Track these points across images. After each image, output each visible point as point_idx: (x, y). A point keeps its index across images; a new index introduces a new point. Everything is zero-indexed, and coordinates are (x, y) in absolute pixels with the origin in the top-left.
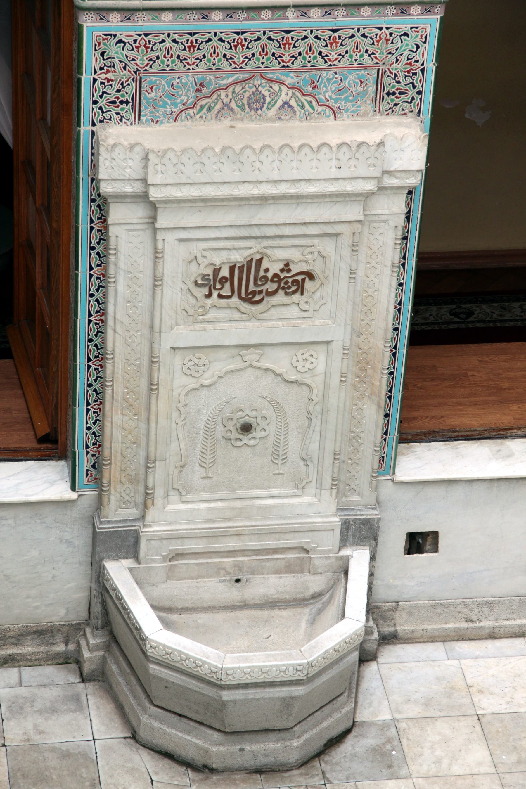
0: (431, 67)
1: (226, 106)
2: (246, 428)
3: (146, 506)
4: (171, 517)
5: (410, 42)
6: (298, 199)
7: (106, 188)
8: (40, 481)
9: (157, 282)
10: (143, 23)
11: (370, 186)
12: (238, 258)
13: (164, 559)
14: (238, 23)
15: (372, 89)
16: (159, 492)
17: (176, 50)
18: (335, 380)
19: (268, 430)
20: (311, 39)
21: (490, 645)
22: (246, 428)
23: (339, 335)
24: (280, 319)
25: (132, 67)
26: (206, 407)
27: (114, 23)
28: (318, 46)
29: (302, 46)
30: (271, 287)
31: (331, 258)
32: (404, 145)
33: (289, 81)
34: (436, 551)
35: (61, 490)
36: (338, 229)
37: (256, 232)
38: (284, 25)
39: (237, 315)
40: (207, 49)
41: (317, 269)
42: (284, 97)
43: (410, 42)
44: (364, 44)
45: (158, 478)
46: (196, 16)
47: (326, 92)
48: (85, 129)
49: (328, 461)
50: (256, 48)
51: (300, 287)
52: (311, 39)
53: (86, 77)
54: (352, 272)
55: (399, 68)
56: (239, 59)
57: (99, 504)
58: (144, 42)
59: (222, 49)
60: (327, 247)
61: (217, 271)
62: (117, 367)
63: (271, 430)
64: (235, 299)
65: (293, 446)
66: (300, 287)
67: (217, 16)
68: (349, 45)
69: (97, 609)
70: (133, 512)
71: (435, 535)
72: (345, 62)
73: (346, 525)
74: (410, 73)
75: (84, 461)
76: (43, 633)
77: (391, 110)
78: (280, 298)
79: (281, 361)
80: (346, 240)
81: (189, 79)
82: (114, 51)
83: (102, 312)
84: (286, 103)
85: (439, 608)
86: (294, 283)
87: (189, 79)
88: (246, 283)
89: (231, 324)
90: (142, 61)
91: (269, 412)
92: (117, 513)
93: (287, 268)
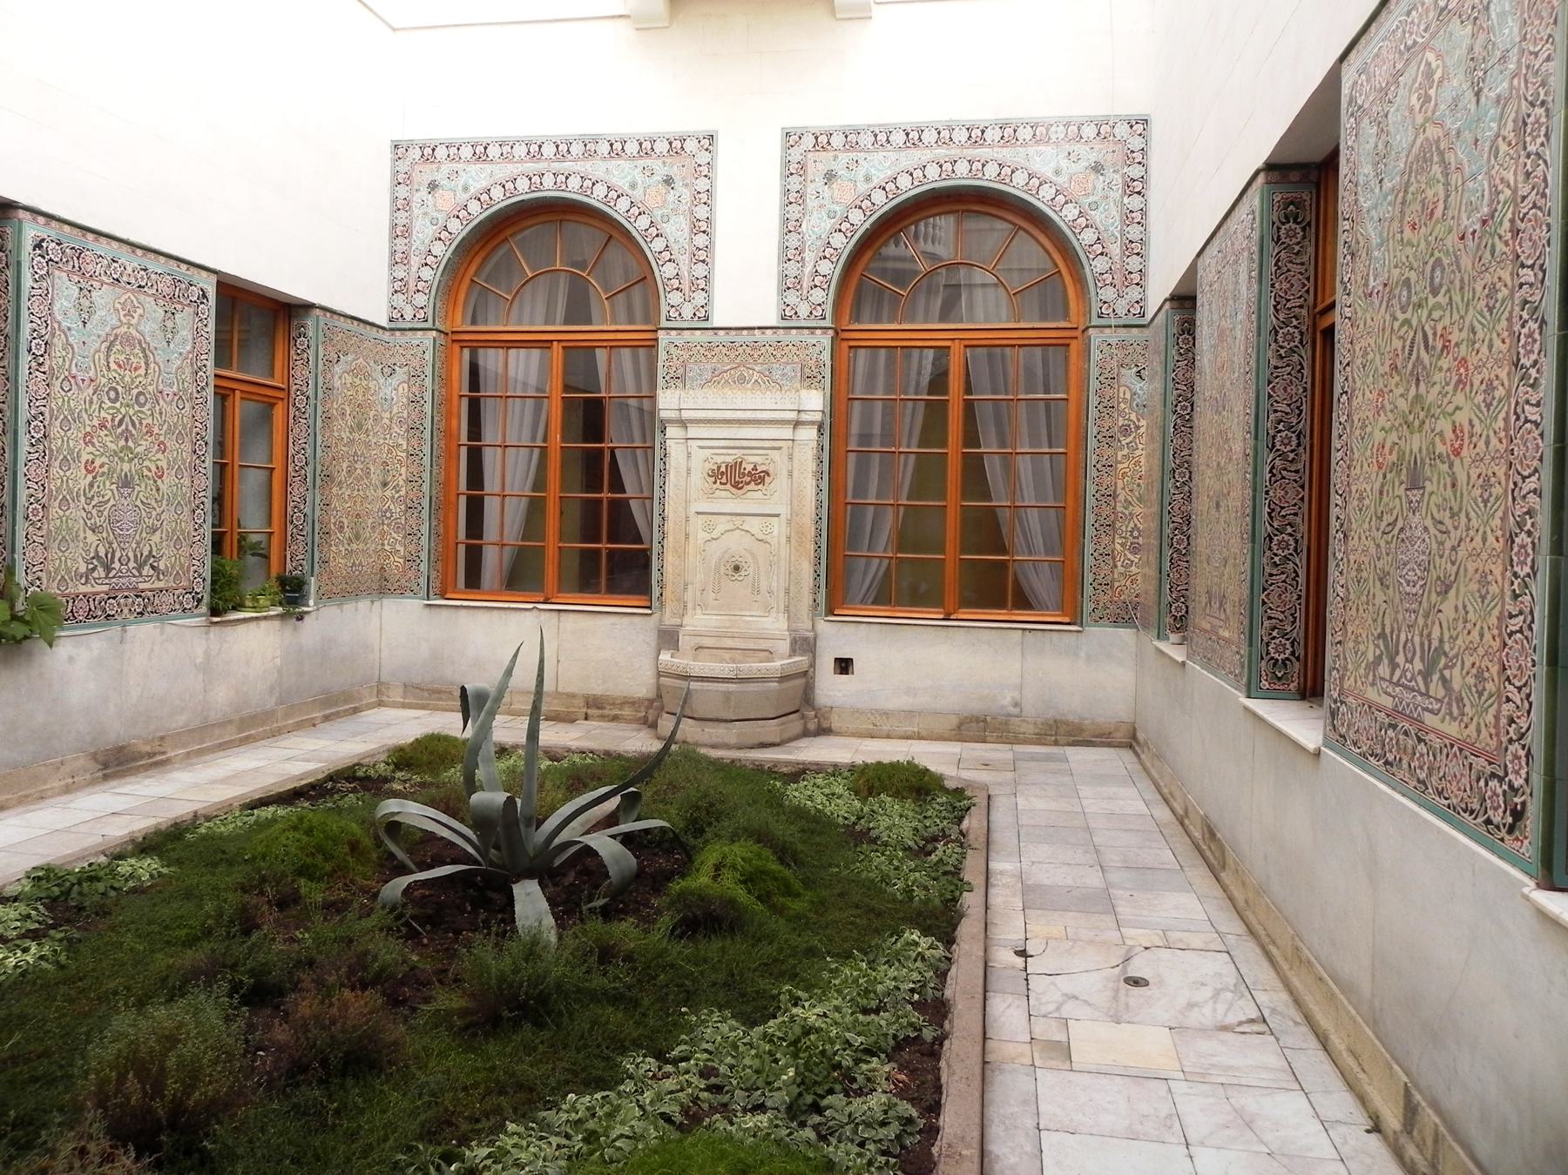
0: (828, 363)
2: (737, 568)
5: (817, 349)
7: (663, 414)
11: (793, 416)
12: (729, 459)
14: (732, 336)
16: (690, 606)
18: (783, 540)
19: (749, 571)
22: (737, 568)
23: (784, 510)
26: (715, 551)
28: (771, 350)
31: (777, 462)
32: (814, 401)
37: (737, 443)
43: (817, 349)
45: (689, 596)
47: (777, 375)
49: (782, 594)
53: (660, 364)
58: (687, 346)
59: (724, 350)
60: (775, 455)
62: (670, 526)
63: (751, 570)
65: (764, 585)
66: (763, 481)
67: (721, 333)
70: (678, 621)
73: (794, 642)
77: (809, 387)
78: (752, 486)
79: (754, 525)
80: (785, 451)
81: (708, 366)
82: (673, 350)
85: (857, 712)
86: (759, 477)
87: (708, 366)
88: (736, 477)
89: (727, 501)
90: (686, 356)
91: (750, 560)
93: (755, 468)
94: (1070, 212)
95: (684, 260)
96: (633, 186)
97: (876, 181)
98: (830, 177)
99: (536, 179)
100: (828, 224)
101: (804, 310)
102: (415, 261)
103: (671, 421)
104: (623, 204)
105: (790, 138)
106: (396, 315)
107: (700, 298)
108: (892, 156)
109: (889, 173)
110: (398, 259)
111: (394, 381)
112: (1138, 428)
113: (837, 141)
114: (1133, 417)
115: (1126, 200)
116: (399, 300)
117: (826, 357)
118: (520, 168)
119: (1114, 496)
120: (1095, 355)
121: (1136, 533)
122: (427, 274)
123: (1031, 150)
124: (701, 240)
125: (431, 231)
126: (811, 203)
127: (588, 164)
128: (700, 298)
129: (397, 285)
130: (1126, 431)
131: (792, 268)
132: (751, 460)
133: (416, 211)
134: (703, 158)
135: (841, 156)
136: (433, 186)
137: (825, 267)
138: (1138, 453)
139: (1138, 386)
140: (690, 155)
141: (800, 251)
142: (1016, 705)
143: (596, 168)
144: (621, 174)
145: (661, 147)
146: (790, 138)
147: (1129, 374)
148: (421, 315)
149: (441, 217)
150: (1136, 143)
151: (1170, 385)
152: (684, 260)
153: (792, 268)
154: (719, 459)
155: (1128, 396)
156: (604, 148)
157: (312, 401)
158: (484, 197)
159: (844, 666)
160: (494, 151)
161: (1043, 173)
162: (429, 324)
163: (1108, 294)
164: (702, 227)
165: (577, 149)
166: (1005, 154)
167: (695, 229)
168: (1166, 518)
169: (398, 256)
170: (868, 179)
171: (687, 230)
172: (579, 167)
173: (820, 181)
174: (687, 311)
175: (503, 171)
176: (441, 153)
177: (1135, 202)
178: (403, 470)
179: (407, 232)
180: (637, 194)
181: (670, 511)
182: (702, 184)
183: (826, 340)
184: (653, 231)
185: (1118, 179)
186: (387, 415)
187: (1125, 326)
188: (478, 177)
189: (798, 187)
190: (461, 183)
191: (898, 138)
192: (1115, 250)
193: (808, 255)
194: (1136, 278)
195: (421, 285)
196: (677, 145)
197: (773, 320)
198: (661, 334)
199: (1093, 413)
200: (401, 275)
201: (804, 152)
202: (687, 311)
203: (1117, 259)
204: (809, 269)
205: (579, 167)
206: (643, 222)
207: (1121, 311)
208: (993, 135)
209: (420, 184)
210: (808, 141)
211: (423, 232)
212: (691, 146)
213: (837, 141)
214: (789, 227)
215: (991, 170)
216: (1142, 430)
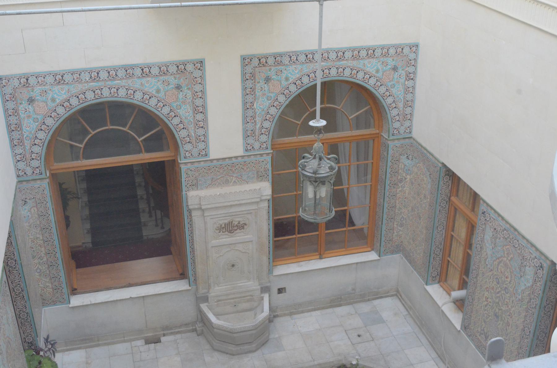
0: (270, 169)
1: (219, 183)
2: (233, 266)
3: (209, 289)
4: (216, 291)
6: (240, 205)
7: (191, 207)
8: (180, 285)
9: (206, 230)
10: (196, 165)
11: (258, 200)
12: (226, 221)
13: (215, 302)
14: (220, 163)
15: (256, 176)
17: (205, 171)
20: (239, 165)
21: (302, 315)
22: (233, 266)
24: (239, 236)
25: (194, 176)
27: (189, 166)
28: (241, 166)
29: (237, 167)
30: (236, 228)
32: (265, 188)
33: (235, 175)
34: (285, 292)
35: (187, 287)
36: (251, 211)
38: (232, 162)
39: (227, 236)
40: (213, 170)
41: (247, 222)
42: (234, 180)
44: (253, 165)
46: (209, 162)
48: (184, 193)
50: (226, 168)
51: (243, 227)
52: (239, 165)
53: (183, 180)
54: (256, 222)
55: (262, 170)
56: (221, 171)
57: (197, 289)
59: (217, 169)
61: (221, 226)
62: (198, 253)
64: (227, 233)
68: (249, 165)
69: (199, 317)
70: (205, 291)
71: (285, 288)
72: (248, 170)
73: (262, 288)
74: (265, 171)
75: (192, 279)
76: (187, 325)
77: (261, 181)
78: (238, 231)
82: (190, 173)
83: (193, 239)
84: (235, 181)
86: (241, 226)
88: (230, 228)
89: (226, 239)
92: (202, 291)
93: (239, 223)
94: (382, 90)
95: (191, 127)
96: (158, 91)
97: (291, 80)
98: (268, 80)
99: (98, 91)
100: (267, 103)
101: (257, 145)
102: (27, 143)
103: (195, 209)
104: (153, 102)
105: (246, 60)
106: (21, 173)
107: (201, 146)
108: (299, 67)
109: (298, 76)
110: (15, 143)
111: (27, 207)
112: (406, 179)
113: (271, 61)
114: (404, 175)
115: (406, 83)
116: (21, 165)
117: (269, 166)
118: (86, 86)
119: (395, 207)
120: (390, 152)
121: (402, 219)
122: (36, 149)
123: (366, 62)
124: (199, 117)
125: (34, 126)
126: (258, 93)
127: (130, 81)
128: (201, 146)
129: (18, 158)
130: (401, 181)
131: (250, 126)
132: (236, 220)
133: (22, 116)
134: (197, 73)
135: (273, 68)
136: (31, 101)
137: (267, 124)
138: (405, 189)
139: (407, 162)
140: (189, 74)
141: (253, 117)
142: (353, 289)
143: (136, 83)
144: (151, 85)
145: (173, 69)
146: (246, 60)
147: (403, 158)
148: (38, 171)
149: (40, 118)
150: (412, 56)
151: (439, 195)
152: (191, 127)
153: (250, 126)
154: (221, 222)
155: (403, 167)
156: (138, 72)
157: (19, 262)
158: (66, 104)
159: (280, 291)
160: (67, 78)
161: (370, 73)
162: (43, 176)
163: (397, 125)
164: (201, 110)
165: (121, 73)
166: (355, 63)
167: (196, 110)
168: (433, 244)
169: (15, 142)
170: (287, 79)
171: (191, 112)
172: (123, 83)
173: (262, 83)
174: (195, 152)
175: (77, 88)
176: (32, 81)
177: (410, 83)
178: (43, 249)
179: (19, 127)
180: (161, 95)
181: (197, 247)
182: (198, 88)
183: (269, 158)
184: (173, 114)
185: (404, 73)
186: (28, 225)
187: (404, 138)
188: (60, 94)
189: (251, 86)
190: (50, 96)
191: (302, 58)
192: (401, 105)
193: (258, 119)
194: (409, 116)
195: (34, 156)
196: (181, 67)
197: (240, 152)
198: (183, 167)
199: (388, 175)
200: (19, 150)
201: (254, 68)
202: (195, 152)
203: (401, 109)
204: (258, 126)
205: (123, 83)
206: (166, 110)
207: (402, 132)
208: (348, 55)
209: (21, 100)
210: (255, 62)
211: (29, 127)
212: (190, 67)
213: (271, 61)
214: (247, 106)
215: (347, 72)
216: (407, 179)
